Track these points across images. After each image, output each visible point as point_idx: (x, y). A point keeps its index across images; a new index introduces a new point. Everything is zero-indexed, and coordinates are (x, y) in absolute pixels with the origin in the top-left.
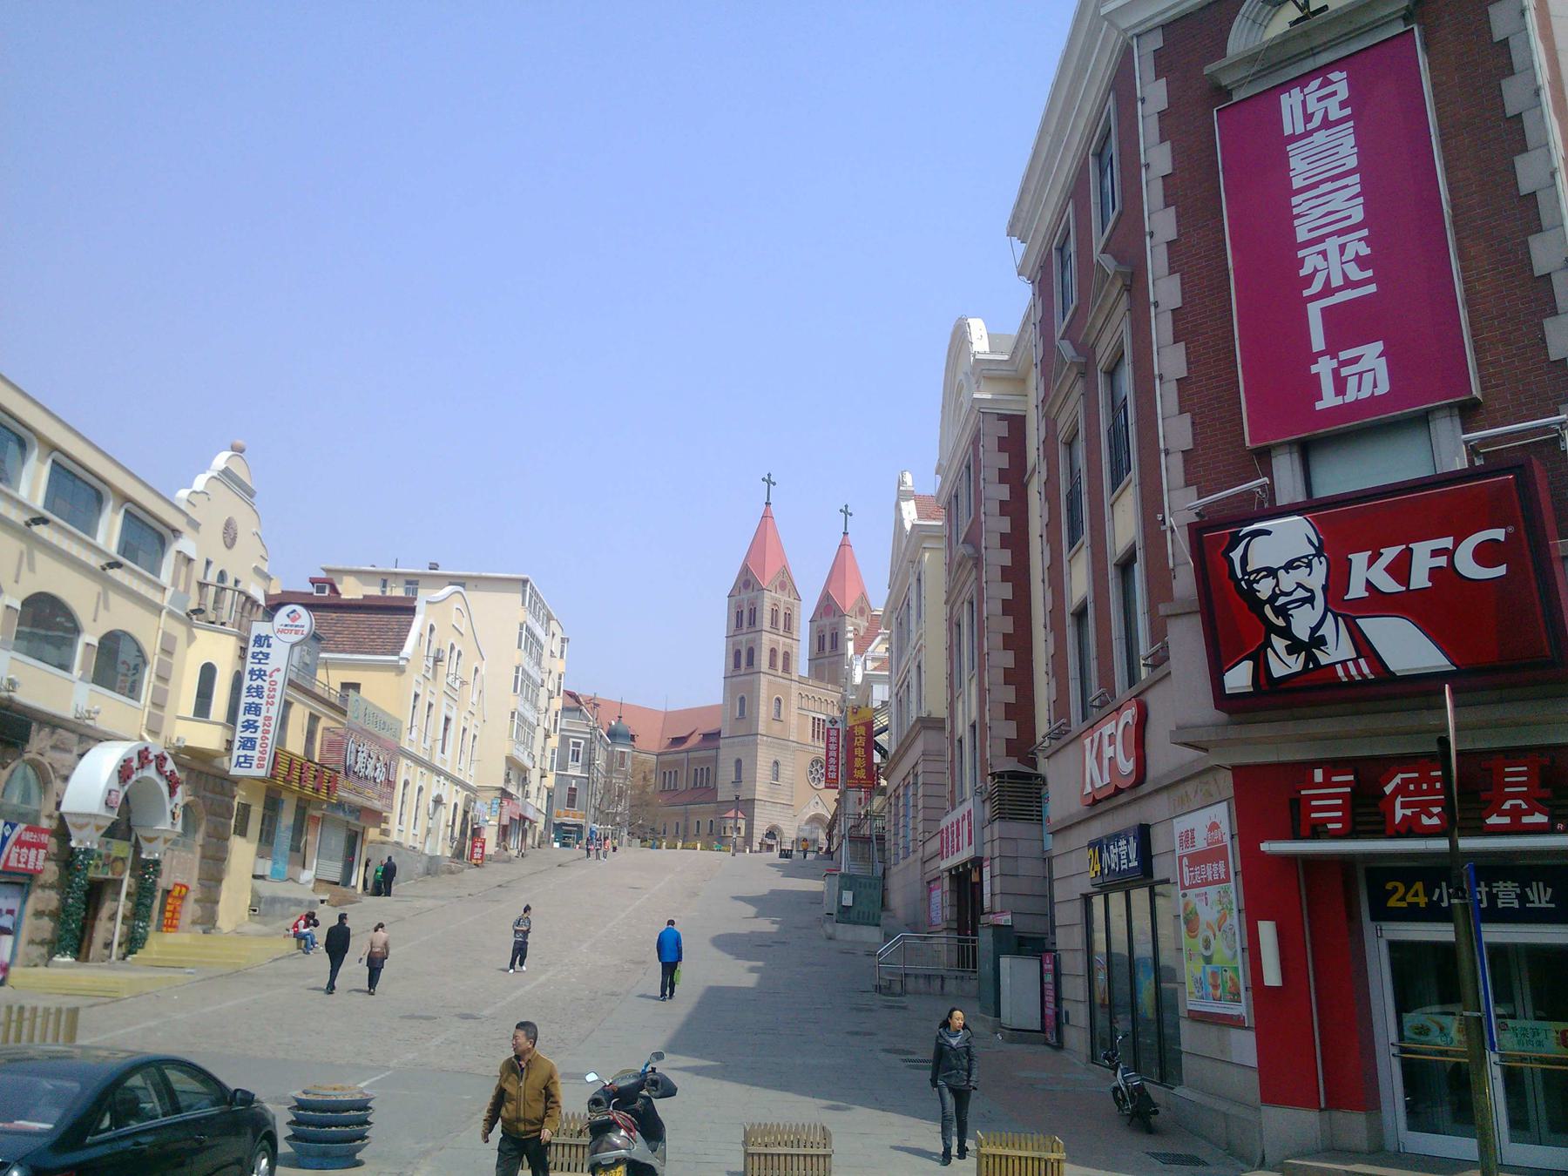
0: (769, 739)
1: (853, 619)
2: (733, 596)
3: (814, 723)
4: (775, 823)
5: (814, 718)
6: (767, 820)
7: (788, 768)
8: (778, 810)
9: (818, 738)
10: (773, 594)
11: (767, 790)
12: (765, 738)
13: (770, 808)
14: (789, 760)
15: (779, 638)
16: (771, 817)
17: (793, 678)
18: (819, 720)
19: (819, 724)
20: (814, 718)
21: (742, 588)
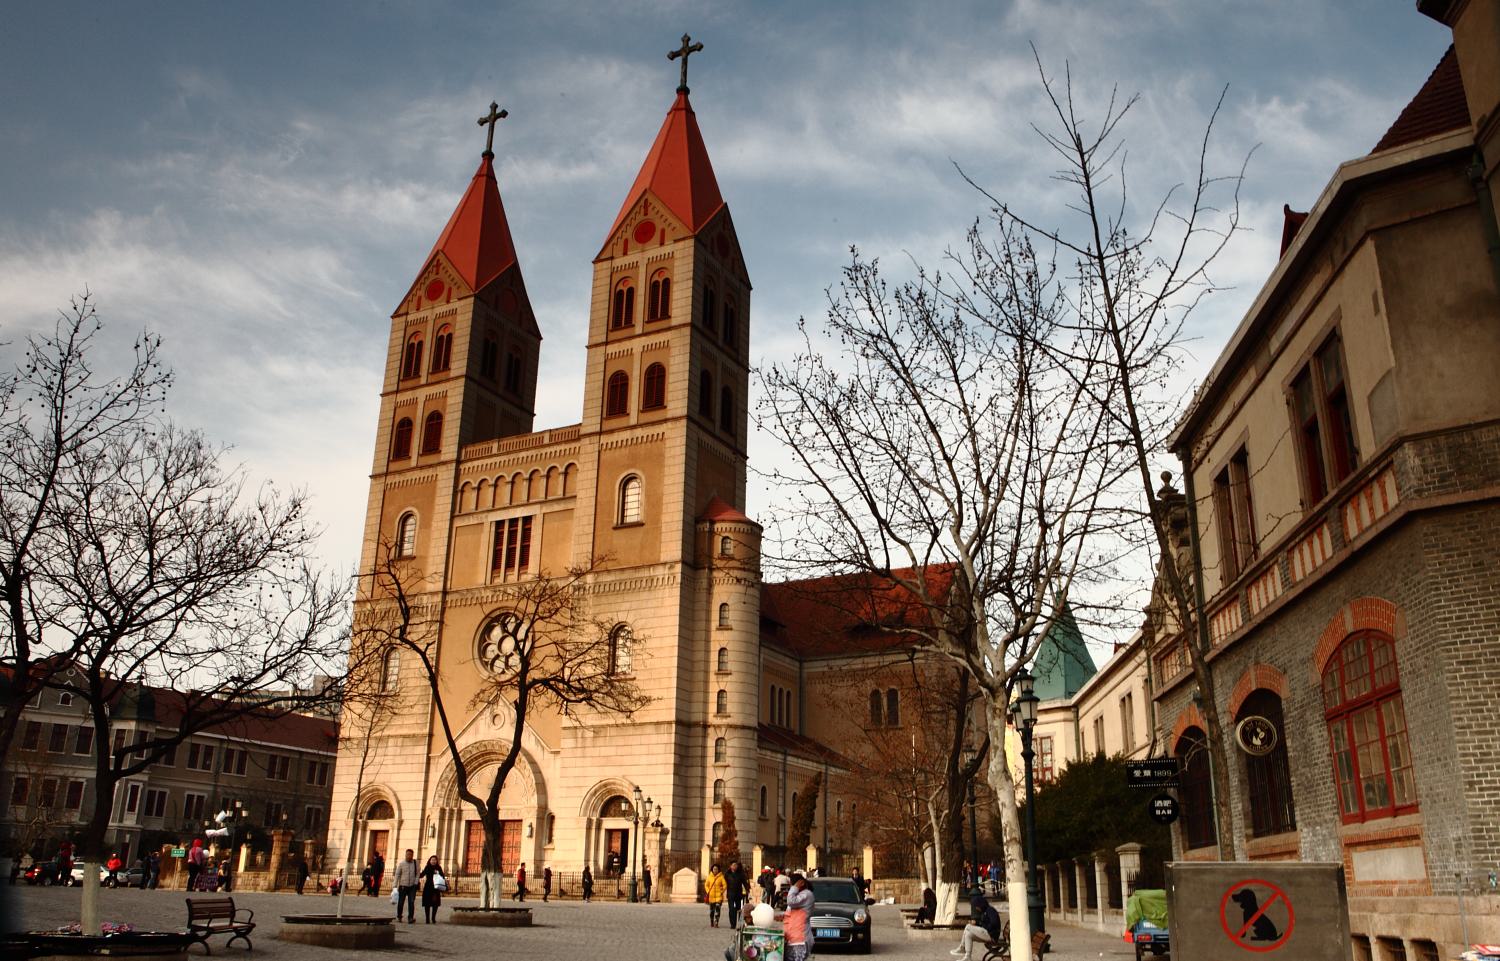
9: (510, 565)
18: (513, 522)
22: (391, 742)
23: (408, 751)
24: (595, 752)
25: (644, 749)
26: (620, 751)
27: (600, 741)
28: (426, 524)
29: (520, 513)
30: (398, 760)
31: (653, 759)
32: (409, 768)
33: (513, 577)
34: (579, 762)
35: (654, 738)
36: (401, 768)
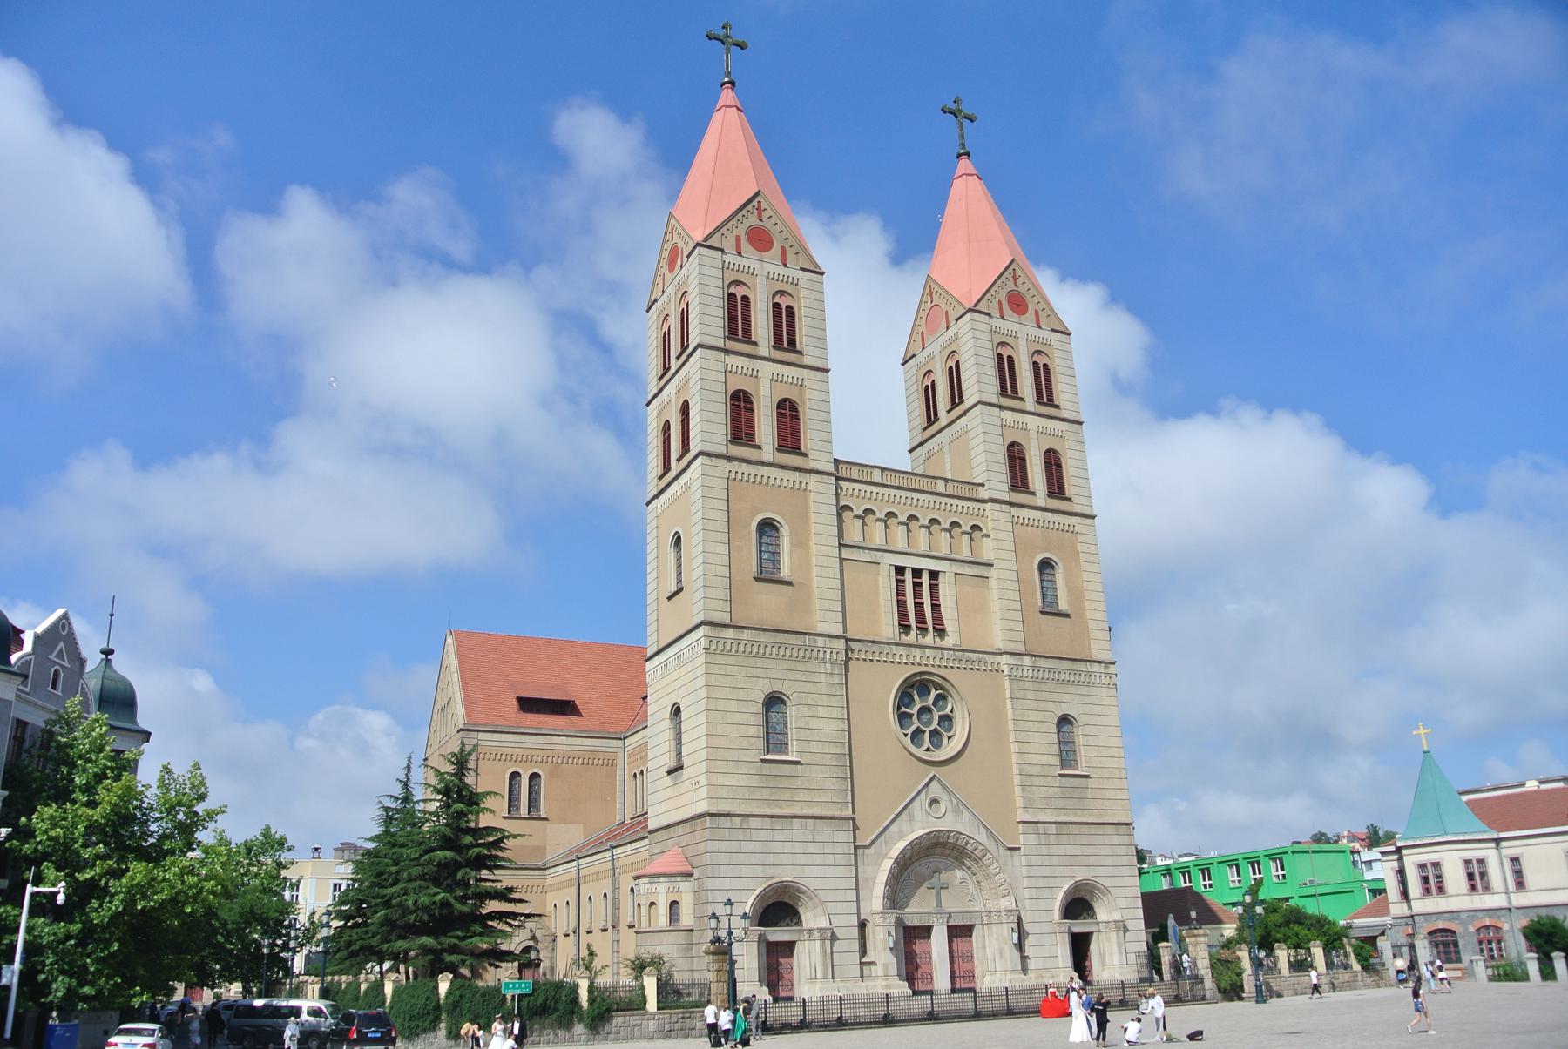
0: (745, 635)
1: (997, 322)
2: (656, 301)
3: (900, 583)
4: (785, 875)
5: (900, 570)
6: (759, 871)
7: (822, 712)
8: (798, 835)
10: (731, 258)
11: (754, 781)
12: (730, 633)
13: (764, 835)
14: (823, 688)
15: (758, 364)
16: (771, 859)
17: (813, 465)
18: (917, 573)
19: (917, 586)
20: (900, 570)
21: (667, 273)
22: (796, 823)
23: (826, 836)
24: (1061, 850)
25: (1108, 850)
26: (1087, 850)
27: (1064, 839)
28: (801, 543)
29: (926, 564)
30: (811, 848)
31: (1119, 861)
32: (829, 859)
33: (929, 639)
34: (1046, 860)
35: (1116, 840)
36: (818, 859)
